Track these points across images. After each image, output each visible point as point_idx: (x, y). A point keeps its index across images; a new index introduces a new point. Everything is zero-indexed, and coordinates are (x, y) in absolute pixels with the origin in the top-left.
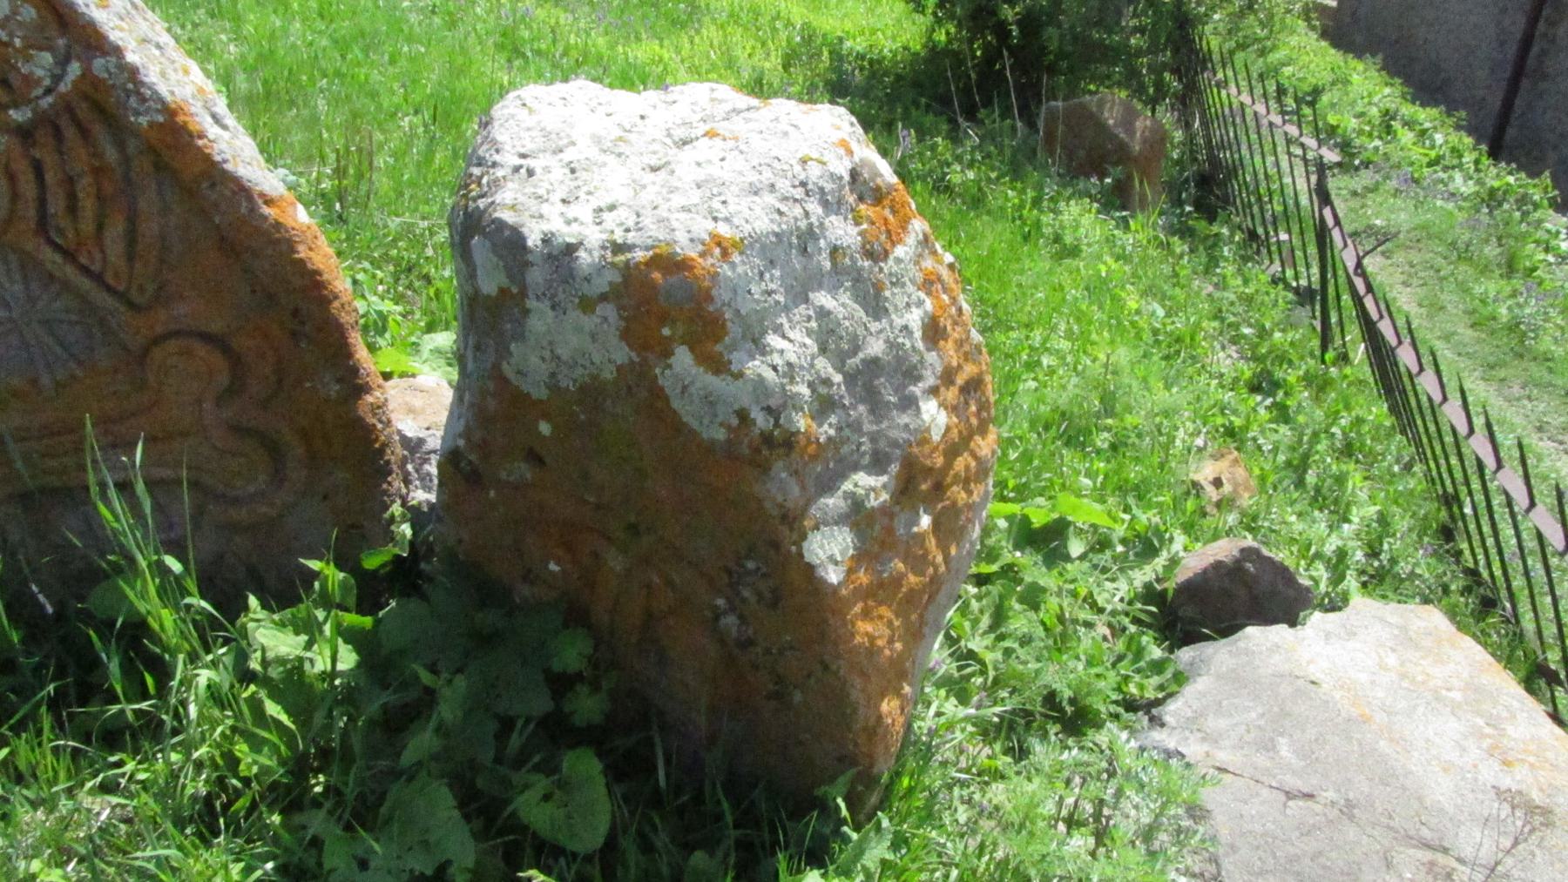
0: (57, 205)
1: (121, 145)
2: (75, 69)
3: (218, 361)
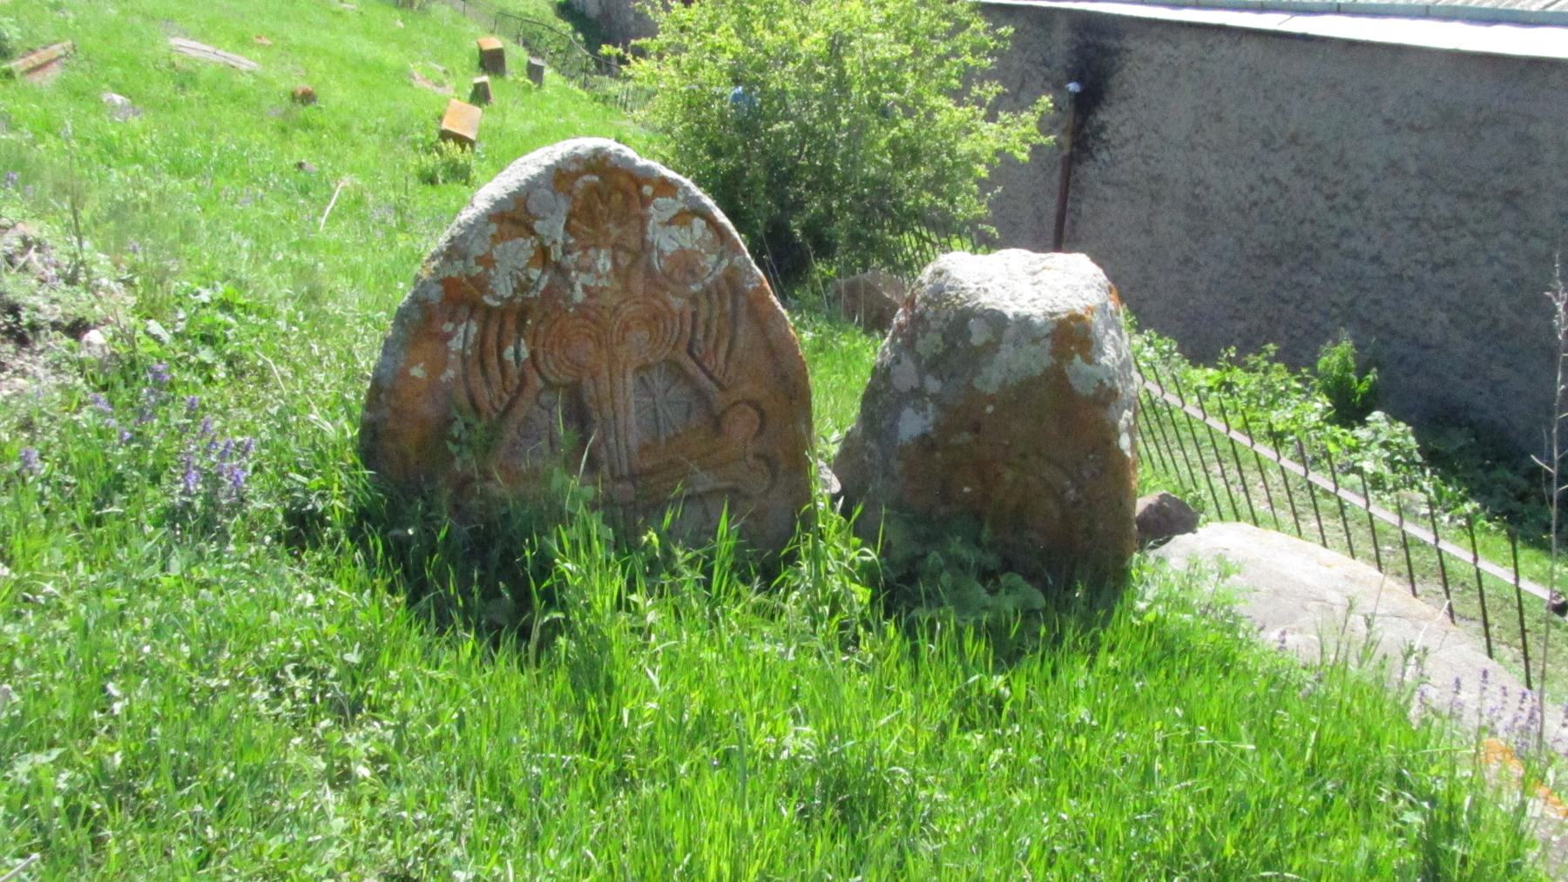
1: (734, 302)
2: (725, 263)
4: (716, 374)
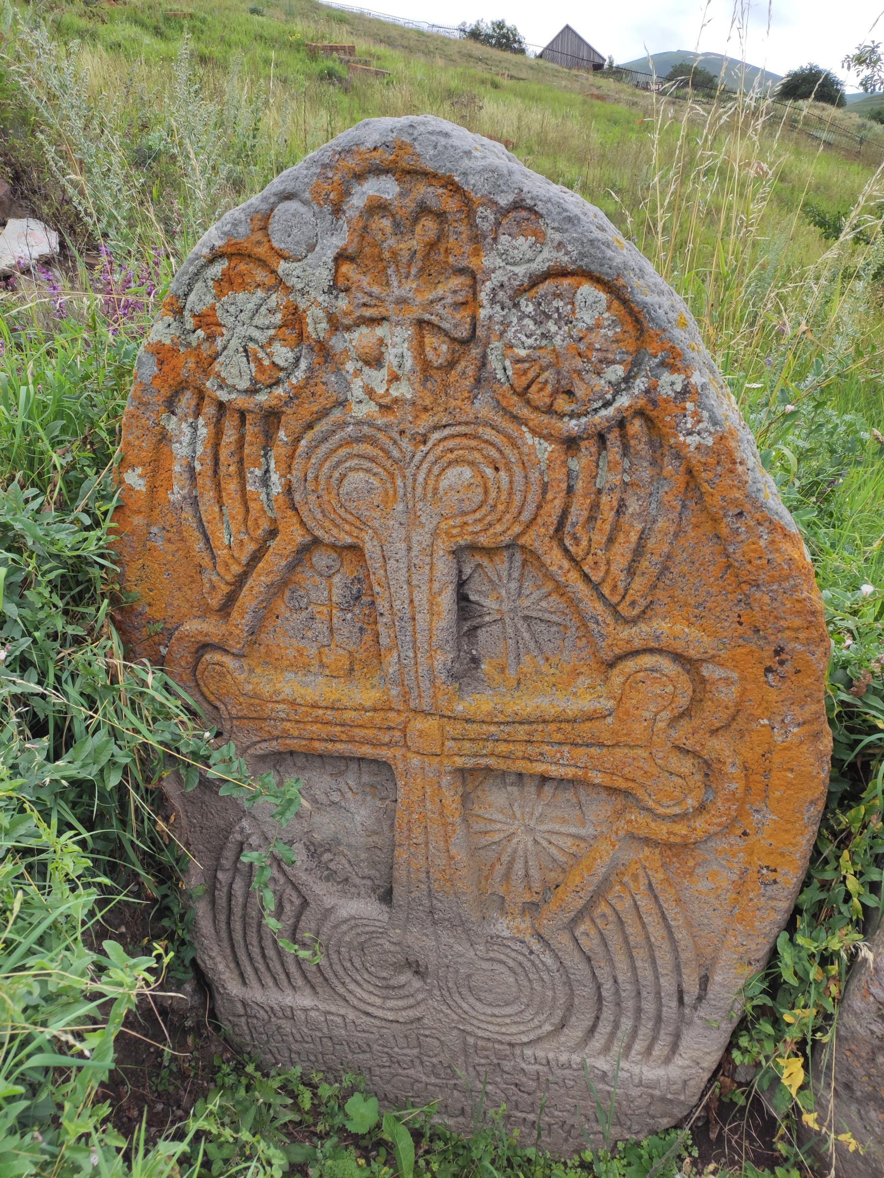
0: (578, 512)
3: (685, 685)
4: (606, 591)
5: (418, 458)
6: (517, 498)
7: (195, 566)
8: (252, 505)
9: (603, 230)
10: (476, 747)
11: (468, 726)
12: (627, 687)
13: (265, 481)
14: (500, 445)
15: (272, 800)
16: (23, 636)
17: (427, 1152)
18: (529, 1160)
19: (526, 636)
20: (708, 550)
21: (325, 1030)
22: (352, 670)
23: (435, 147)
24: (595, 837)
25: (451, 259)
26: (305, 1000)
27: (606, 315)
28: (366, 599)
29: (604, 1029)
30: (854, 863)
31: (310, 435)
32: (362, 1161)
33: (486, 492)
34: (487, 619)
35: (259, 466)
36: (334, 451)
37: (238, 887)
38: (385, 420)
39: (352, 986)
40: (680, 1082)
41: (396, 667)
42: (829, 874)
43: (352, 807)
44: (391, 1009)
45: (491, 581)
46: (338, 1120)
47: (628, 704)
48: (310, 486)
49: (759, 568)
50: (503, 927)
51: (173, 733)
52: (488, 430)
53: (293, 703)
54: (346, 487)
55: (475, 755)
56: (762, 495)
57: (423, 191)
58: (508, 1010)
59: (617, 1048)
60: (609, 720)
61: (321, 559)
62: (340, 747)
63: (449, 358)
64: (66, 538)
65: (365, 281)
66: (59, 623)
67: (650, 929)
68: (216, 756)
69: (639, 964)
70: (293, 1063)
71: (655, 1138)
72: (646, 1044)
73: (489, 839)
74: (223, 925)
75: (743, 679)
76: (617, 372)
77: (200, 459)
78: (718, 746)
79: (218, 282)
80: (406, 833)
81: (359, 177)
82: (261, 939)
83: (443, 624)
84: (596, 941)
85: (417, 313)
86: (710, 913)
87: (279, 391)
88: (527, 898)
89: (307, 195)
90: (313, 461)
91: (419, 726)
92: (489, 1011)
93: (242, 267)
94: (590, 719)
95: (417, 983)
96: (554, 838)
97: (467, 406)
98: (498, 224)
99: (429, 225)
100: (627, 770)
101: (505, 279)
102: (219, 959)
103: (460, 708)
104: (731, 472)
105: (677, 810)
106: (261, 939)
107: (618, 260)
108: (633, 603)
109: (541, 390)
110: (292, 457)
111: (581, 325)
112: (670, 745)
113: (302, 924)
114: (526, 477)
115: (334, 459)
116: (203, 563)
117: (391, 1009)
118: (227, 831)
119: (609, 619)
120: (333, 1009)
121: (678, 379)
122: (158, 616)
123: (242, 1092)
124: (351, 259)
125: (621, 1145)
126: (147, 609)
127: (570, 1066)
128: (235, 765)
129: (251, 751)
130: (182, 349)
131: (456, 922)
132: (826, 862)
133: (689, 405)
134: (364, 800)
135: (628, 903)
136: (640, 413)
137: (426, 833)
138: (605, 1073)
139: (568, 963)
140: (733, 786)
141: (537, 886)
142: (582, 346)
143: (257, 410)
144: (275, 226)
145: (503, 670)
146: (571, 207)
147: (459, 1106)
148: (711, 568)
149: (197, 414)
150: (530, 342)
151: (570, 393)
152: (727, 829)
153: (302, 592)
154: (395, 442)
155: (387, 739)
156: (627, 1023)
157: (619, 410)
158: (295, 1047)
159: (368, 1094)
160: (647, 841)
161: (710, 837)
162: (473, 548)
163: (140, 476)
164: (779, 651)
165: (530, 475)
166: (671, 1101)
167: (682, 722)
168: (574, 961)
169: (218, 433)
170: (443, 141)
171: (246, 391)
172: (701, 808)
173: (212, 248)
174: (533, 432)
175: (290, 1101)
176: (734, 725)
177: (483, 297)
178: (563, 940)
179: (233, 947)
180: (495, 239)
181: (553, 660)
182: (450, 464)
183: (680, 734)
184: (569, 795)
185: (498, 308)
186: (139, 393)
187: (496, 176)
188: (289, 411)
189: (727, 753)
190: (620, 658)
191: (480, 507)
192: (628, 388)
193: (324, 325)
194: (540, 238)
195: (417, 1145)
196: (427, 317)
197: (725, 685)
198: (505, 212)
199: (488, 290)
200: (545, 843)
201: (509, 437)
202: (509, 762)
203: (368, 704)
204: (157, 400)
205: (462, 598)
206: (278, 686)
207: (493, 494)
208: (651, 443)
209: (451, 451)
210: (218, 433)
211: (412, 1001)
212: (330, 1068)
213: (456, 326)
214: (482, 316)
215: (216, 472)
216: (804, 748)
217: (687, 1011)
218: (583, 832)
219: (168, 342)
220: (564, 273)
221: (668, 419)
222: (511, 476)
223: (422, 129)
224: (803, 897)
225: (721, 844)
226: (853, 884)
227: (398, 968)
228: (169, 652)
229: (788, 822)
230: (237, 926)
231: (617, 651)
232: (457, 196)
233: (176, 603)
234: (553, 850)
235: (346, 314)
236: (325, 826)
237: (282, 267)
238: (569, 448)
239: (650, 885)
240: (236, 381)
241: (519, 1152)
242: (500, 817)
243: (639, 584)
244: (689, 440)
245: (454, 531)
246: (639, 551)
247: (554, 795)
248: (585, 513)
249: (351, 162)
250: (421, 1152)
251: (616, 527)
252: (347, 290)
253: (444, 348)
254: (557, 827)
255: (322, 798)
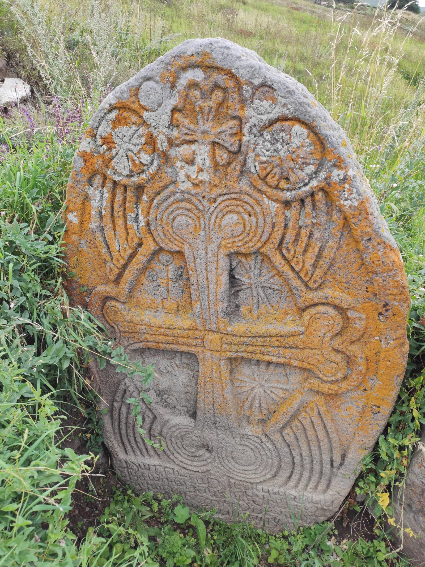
0: (290, 237)
3: (339, 320)
4: (302, 275)
5: (212, 209)
6: (260, 230)
7: (102, 260)
8: (130, 231)
9: (306, 97)
10: (237, 348)
11: (234, 338)
12: (311, 321)
13: (136, 219)
14: (252, 204)
15: (141, 374)
16: (21, 296)
17: (211, 530)
18: (259, 535)
19: (263, 295)
20: (353, 256)
21: (164, 475)
22: (178, 310)
23: (223, 54)
24: (293, 390)
25: (230, 112)
26: (154, 461)
27: (307, 140)
28: (185, 277)
29: (295, 477)
30: (416, 403)
31: (158, 198)
32: (182, 535)
33: (245, 227)
34: (244, 287)
35: (134, 212)
36: (170, 206)
37: (124, 410)
38: (196, 191)
39: (177, 455)
40: (330, 501)
41: (200, 310)
42: (404, 408)
43: (177, 374)
44: (195, 466)
45: (246, 269)
46: (171, 517)
47: (311, 329)
48: (159, 223)
49: (378, 265)
50: (248, 430)
51: (93, 342)
52: (246, 196)
53: (150, 326)
54: (176, 224)
55: (237, 352)
56: (381, 230)
57: (216, 77)
58: (250, 468)
59: (301, 486)
60: (302, 336)
61: (164, 257)
62: (172, 347)
63: (228, 161)
64: (41, 247)
65: (187, 122)
66: (38, 289)
67: (318, 433)
68: (114, 353)
69: (312, 448)
70: (149, 490)
71: (318, 525)
72: (315, 484)
73: (242, 390)
74: (116, 427)
75: (367, 318)
76: (311, 169)
77: (105, 209)
78: (354, 349)
79: (113, 121)
80: (203, 387)
81: (184, 69)
82: (134, 433)
83: (223, 290)
84: (293, 437)
85: (212, 138)
86: (347, 426)
87: (143, 176)
88: (260, 417)
89: (158, 78)
90: (160, 210)
91: (210, 337)
92: (241, 468)
93: (125, 114)
94: (293, 336)
95: (207, 455)
96: (274, 390)
97: (236, 185)
98: (254, 94)
99: (218, 95)
100: (310, 359)
101: (256, 122)
102: (114, 442)
103: (230, 329)
104: (366, 218)
105: (333, 379)
106: (134, 433)
107: (313, 113)
108: (315, 282)
109: (273, 177)
110: (150, 208)
111: (294, 145)
112: (331, 348)
113: (154, 427)
114: (264, 220)
115: (170, 209)
116: (107, 259)
117: (195, 466)
118: (118, 384)
119: (304, 289)
120: (168, 465)
121: (342, 173)
122: (85, 283)
123: (126, 503)
124: (180, 111)
125: (301, 529)
126: (79, 280)
127: (279, 493)
128: (123, 357)
129: (130, 347)
130: (96, 155)
131: (227, 428)
132: (403, 402)
133: (347, 186)
134: (183, 371)
135: (308, 420)
136: (322, 189)
137: (213, 387)
138: (295, 497)
139: (279, 447)
140: (361, 368)
141: (265, 412)
142: (294, 156)
143: (132, 185)
144: (141, 94)
145: (251, 311)
146: (290, 86)
147: (227, 510)
148: (354, 265)
149: (103, 186)
150: (268, 153)
151: (287, 179)
152: (357, 387)
153: (154, 273)
154: (200, 202)
155: (194, 343)
156: (306, 475)
157: (311, 188)
158: (150, 482)
159: (185, 504)
160: (318, 392)
161: (348, 391)
162: (238, 253)
163: (75, 216)
164: (386, 305)
165: (267, 219)
166: (326, 510)
167: (337, 337)
168: (282, 446)
169: (114, 196)
170: (226, 51)
171: (127, 176)
172: (345, 378)
173: (111, 104)
174: (269, 198)
175: (149, 509)
176: (362, 340)
177: (245, 131)
178: (278, 436)
179: (121, 436)
180: (252, 102)
181: (275, 307)
182: (227, 213)
183: (336, 343)
184: (281, 370)
185: (252, 136)
186: (74, 176)
187: (254, 70)
188: (148, 186)
189: (358, 352)
190: (308, 307)
191: (241, 234)
192: (316, 177)
193: (166, 144)
194: (274, 101)
195: (207, 527)
196: (217, 140)
197: (359, 320)
198: (257, 88)
199: (248, 128)
200: (269, 392)
201: (256, 200)
202: (253, 355)
203: (186, 327)
204: (84, 179)
205: (232, 277)
206: (143, 317)
207: (248, 228)
208: (327, 204)
209: (228, 206)
210: (114, 196)
211: (205, 463)
212: (166, 492)
213: (231, 145)
214: (244, 140)
215: (112, 215)
216: (396, 350)
217: (335, 470)
218: (287, 387)
219: (88, 151)
220: (286, 119)
221: (336, 192)
222: (257, 219)
223: (216, 45)
224: (392, 419)
225: (354, 394)
226: (416, 413)
227: (198, 447)
228: (90, 300)
229: (386, 385)
230: (123, 427)
231: (307, 304)
232: (233, 80)
233: (93, 277)
234: (273, 396)
235: (177, 138)
236: (165, 382)
237: (145, 114)
238: (286, 205)
239: (319, 412)
240: (122, 171)
241: (254, 531)
242: (248, 380)
243: (318, 272)
244: (346, 203)
245: (229, 245)
246: (319, 256)
247: (274, 370)
248: (293, 238)
249: (181, 62)
250: (209, 530)
251: (308, 245)
252: (177, 126)
253: (225, 156)
254: (275, 385)
255: (163, 369)
